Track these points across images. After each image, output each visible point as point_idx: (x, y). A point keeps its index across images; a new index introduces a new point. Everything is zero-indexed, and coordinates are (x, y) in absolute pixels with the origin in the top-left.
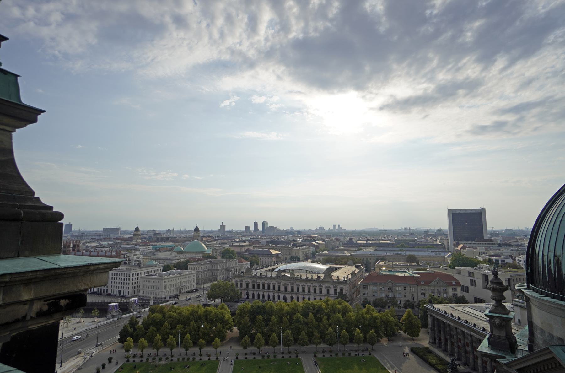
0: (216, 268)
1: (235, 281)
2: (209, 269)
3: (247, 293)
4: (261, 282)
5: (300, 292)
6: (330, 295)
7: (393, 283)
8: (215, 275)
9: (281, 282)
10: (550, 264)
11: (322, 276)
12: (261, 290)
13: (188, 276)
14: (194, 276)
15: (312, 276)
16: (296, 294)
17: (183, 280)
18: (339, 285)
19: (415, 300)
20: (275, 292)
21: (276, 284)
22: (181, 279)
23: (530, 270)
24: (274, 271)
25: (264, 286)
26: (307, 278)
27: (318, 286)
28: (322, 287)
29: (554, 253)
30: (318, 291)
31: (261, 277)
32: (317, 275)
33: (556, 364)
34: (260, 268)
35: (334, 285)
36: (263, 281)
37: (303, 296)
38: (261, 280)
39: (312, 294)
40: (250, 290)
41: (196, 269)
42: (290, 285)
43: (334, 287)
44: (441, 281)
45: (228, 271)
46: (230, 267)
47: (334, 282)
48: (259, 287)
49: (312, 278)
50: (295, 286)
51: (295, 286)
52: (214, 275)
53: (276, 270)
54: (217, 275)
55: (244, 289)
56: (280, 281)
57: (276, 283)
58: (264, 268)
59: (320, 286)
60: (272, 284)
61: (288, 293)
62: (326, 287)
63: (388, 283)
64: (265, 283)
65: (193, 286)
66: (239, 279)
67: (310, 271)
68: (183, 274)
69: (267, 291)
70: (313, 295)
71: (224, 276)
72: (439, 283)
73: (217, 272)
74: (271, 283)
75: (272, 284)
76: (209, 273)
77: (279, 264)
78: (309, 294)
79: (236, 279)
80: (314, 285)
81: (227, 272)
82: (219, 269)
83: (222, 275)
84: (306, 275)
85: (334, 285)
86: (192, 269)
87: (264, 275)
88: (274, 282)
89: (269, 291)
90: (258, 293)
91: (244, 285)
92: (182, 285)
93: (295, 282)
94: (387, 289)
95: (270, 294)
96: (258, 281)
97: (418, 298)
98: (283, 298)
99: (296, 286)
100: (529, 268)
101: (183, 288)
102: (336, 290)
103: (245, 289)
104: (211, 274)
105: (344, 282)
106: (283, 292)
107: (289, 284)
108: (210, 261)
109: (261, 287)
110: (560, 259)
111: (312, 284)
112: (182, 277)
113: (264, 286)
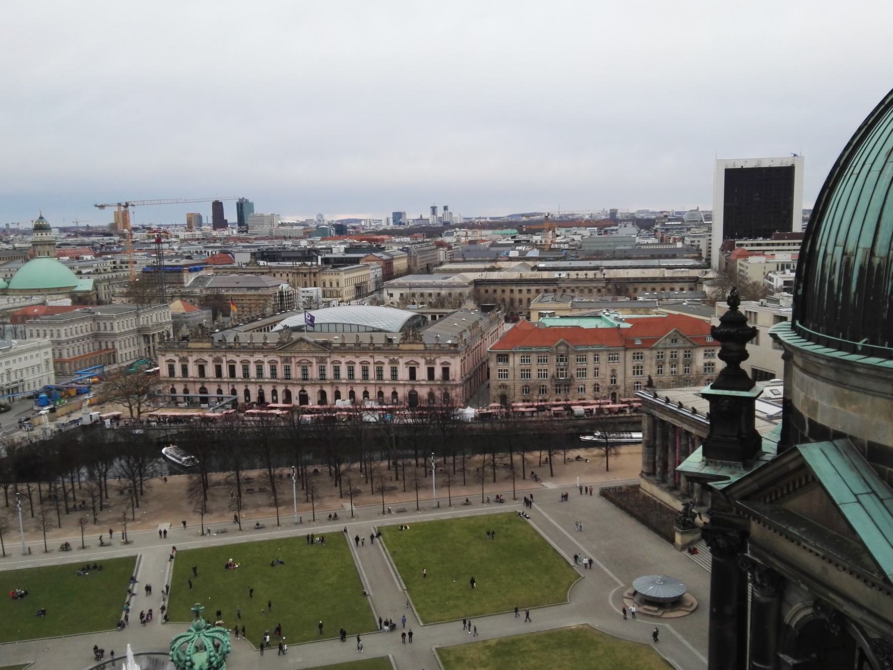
1: (166, 361)
2: (90, 333)
3: (201, 389)
5: (344, 379)
6: (418, 383)
7: (568, 347)
9: (291, 357)
10: (834, 273)
11: (396, 338)
12: (240, 380)
13: (28, 355)
14: (46, 353)
15: (372, 338)
16: (332, 384)
17: (14, 367)
19: (618, 383)
20: (276, 382)
22: (8, 363)
23: (801, 290)
24: (273, 330)
25: (246, 369)
26: (358, 344)
27: (386, 361)
29: (845, 247)
30: (387, 374)
31: (237, 348)
32: (383, 334)
33: (807, 478)
34: (234, 324)
35: (428, 358)
36: (244, 357)
38: (238, 356)
41: (52, 336)
42: (314, 364)
43: (427, 363)
44: (681, 335)
45: (145, 336)
46: (150, 324)
47: (426, 349)
48: (232, 373)
49: (372, 344)
52: (105, 350)
53: (279, 327)
54: (113, 346)
55: (192, 379)
57: (279, 360)
58: (245, 324)
59: (393, 362)
60: (269, 362)
61: (312, 384)
62: (406, 363)
63: (557, 347)
64: (249, 362)
66: (176, 355)
67: (366, 327)
68: (12, 351)
69: (256, 383)
70: (375, 384)
71: (132, 349)
72: (676, 340)
73: (112, 339)
75: (269, 362)
76: (91, 345)
77: (286, 312)
78: (364, 382)
79: (167, 355)
80: (376, 361)
81: (142, 339)
82: (117, 332)
83: (130, 346)
84: (357, 336)
85: (428, 358)
86: (38, 336)
87: (244, 338)
88: (272, 357)
90: (231, 388)
91: (193, 371)
93: (328, 355)
94: (555, 360)
95: (263, 388)
96: (231, 356)
97: (625, 377)
98: (298, 395)
99: (332, 366)
100: (801, 285)
102: (431, 372)
103: (196, 380)
105: (452, 348)
107: (314, 361)
108: (89, 312)
109: (239, 372)
110: (853, 258)
111: (371, 357)
112: (11, 359)
113: (246, 369)
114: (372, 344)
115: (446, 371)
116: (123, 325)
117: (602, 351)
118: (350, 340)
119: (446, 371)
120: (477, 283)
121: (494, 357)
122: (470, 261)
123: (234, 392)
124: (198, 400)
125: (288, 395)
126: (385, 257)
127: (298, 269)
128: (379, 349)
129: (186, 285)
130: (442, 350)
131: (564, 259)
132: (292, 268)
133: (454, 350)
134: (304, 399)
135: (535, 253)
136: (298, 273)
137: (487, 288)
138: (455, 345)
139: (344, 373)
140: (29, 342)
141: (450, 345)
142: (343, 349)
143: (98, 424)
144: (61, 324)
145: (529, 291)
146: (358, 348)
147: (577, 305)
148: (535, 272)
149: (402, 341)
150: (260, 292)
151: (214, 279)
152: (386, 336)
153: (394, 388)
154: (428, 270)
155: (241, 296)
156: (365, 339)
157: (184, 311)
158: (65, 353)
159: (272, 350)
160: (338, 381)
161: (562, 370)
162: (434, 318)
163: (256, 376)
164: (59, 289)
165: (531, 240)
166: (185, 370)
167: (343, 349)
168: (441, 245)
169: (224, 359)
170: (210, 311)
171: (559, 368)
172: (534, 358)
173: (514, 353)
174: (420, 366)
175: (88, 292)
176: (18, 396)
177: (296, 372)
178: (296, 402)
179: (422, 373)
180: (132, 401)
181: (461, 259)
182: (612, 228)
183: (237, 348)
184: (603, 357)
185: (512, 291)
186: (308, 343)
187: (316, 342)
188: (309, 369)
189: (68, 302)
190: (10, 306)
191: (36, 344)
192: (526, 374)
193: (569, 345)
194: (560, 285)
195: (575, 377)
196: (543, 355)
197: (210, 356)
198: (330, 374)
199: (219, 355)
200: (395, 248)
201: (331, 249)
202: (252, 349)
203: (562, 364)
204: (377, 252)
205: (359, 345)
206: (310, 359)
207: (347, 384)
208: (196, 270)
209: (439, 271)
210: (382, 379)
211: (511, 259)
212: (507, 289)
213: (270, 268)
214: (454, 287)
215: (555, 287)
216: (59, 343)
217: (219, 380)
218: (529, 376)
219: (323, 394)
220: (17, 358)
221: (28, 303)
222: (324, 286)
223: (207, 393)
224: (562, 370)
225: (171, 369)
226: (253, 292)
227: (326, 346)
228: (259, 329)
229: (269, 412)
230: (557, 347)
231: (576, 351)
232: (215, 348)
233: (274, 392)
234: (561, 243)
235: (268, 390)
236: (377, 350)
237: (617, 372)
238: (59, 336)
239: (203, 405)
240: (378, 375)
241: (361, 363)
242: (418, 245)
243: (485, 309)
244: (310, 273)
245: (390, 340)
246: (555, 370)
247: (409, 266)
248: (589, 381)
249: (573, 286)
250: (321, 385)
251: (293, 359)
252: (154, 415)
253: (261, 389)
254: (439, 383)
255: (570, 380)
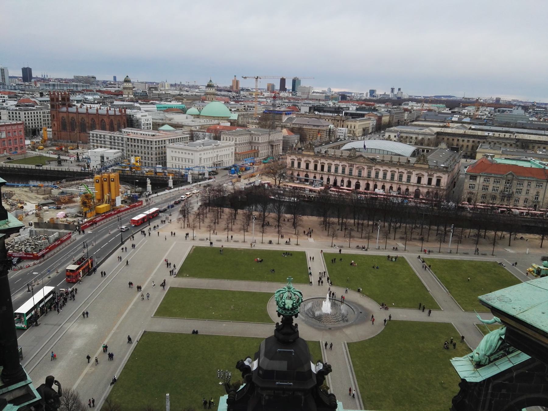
0: (257, 141)
3: (306, 175)
4: (326, 162)
8: (255, 149)
9: (354, 164)
11: (413, 160)
12: (325, 173)
13: (225, 149)
14: (232, 149)
15: (399, 159)
16: (374, 180)
17: (220, 154)
18: (436, 173)
19: (539, 200)
21: (347, 167)
22: (217, 151)
25: (329, 168)
27: (405, 172)
28: (411, 173)
30: (405, 179)
35: (430, 173)
37: (382, 184)
38: (327, 161)
39: (396, 182)
40: (310, 172)
41: (236, 141)
43: (429, 175)
48: (322, 169)
49: (399, 162)
50: (373, 170)
51: (373, 170)
54: (258, 149)
55: (302, 170)
56: (353, 163)
57: (347, 165)
58: (325, 145)
60: (342, 166)
62: (417, 174)
65: (231, 161)
67: (392, 152)
68: (219, 146)
69: (334, 175)
70: (397, 183)
73: (258, 145)
74: (341, 164)
75: (342, 166)
79: (292, 156)
80: (400, 171)
81: (270, 146)
82: (260, 141)
84: (391, 157)
85: (430, 173)
86: (227, 140)
87: (331, 152)
89: (336, 174)
90: (321, 176)
91: (303, 165)
92: (219, 160)
93: (374, 165)
94: (504, 182)
96: (323, 160)
97: (544, 197)
99: (375, 171)
101: (220, 164)
104: (250, 148)
105: (445, 169)
106: (357, 177)
107: (366, 167)
109: (326, 169)
111: (397, 169)
112: (219, 150)
113: (329, 168)
114: (399, 162)
115: (439, 181)
116: (263, 139)
117: (534, 180)
118: (387, 159)
119: (439, 181)
120: (438, 134)
121: (469, 176)
122: (428, 121)
123: (322, 178)
124: (304, 180)
125: (349, 184)
126: (379, 115)
127: (335, 118)
128: (403, 165)
129: (283, 121)
130: (439, 170)
131: (485, 124)
132: (332, 116)
133: (445, 170)
134: (358, 186)
135: (467, 120)
136: (335, 120)
137: (444, 137)
138: (447, 168)
139: (381, 175)
140: (225, 143)
141: (444, 167)
142: (383, 163)
143: (262, 185)
144: (237, 136)
145: (468, 141)
146: (391, 164)
147: (505, 152)
148: (471, 131)
149: (416, 162)
150: (319, 128)
151: (297, 121)
152: (407, 159)
153: (408, 187)
154: (398, 124)
155: (310, 129)
156: (395, 159)
157: (287, 134)
158: (237, 149)
159: (345, 159)
160: (377, 179)
161: (507, 188)
162: (428, 151)
163: (334, 172)
164: (223, 117)
165: (461, 112)
166: (299, 164)
167: (383, 163)
168: (406, 110)
169: (319, 161)
170: (299, 136)
171: (506, 187)
172: (492, 180)
173: (481, 176)
174: (424, 177)
175: (236, 120)
176: (220, 168)
177: (355, 172)
178: (353, 187)
179: (424, 181)
180: (277, 176)
181: (424, 119)
182: (502, 109)
183: (325, 156)
184: (533, 184)
185: (458, 140)
186: (364, 158)
187: (368, 158)
188: (362, 171)
189: (228, 124)
190: (205, 124)
191: (226, 144)
192: (485, 188)
193: (515, 175)
194: (488, 140)
195: (515, 193)
196: (498, 179)
197: (313, 159)
198: (373, 175)
199: (317, 159)
200: (383, 110)
201: (349, 108)
202: (334, 158)
203: (508, 185)
204: (374, 111)
205: (392, 162)
206: (364, 166)
207: (381, 181)
208: (288, 114)
209: (412, 125)
210: (401, 181)
211: (453, 122)
212: (456, 139)
213: (320, 116)
214: (427, 135)
215: (484, 140)
216: (236, 144)
217: (315, 171)
218: (487, 189)
219: (368, 185)
220: (221, 150)
221: (212, 123)
222: (347, 127)
223: (308, 177)
224: (507, 188)
225: (293, 163)
226: (316, 128)
227: (373, 160)
228: (333, 148)
229: (341, 190)
230: (507, 175)
231: (519, 179)
232: (316, 156)
233: (342, 181)
234: (480, 115)
235: (339, 180)
236: (401, 165)
237: (540, 194)
238: (236, 141)
239: (306, 183)
240: (400, 179)
241: (391, 171)
242: (395, 110)
243: (453, 149)
244: (341, 120)
245: (409, 161)
246: (503, 188)
247: (389, 120)
248: (523, 196)
249: (495, 141)
250: (368, 180)
251: (355, 165)
252: (286, 185)
253: (336, 179)
254: (433, 187)
255: (511, 194)
